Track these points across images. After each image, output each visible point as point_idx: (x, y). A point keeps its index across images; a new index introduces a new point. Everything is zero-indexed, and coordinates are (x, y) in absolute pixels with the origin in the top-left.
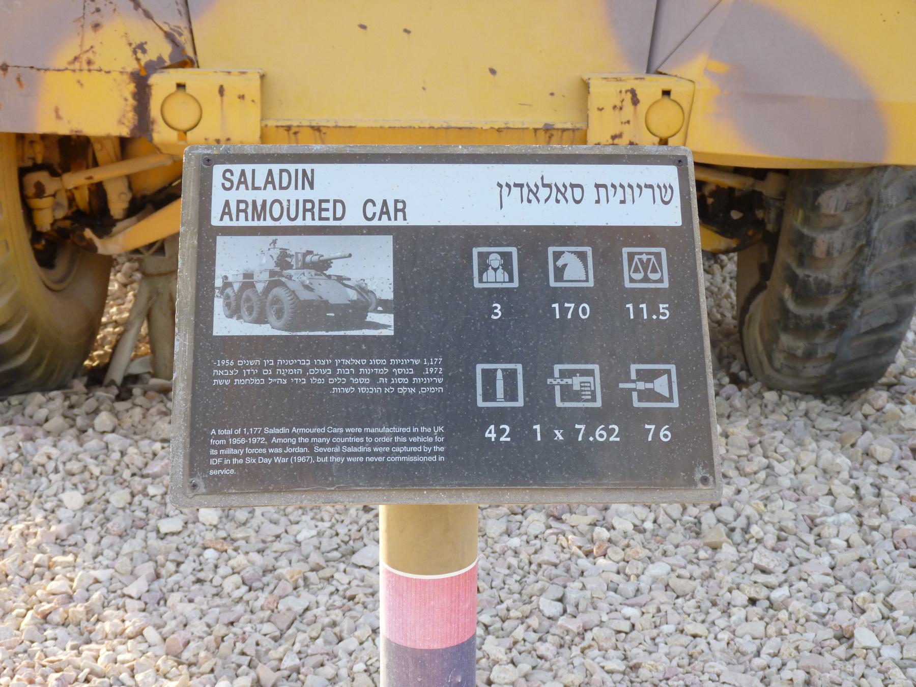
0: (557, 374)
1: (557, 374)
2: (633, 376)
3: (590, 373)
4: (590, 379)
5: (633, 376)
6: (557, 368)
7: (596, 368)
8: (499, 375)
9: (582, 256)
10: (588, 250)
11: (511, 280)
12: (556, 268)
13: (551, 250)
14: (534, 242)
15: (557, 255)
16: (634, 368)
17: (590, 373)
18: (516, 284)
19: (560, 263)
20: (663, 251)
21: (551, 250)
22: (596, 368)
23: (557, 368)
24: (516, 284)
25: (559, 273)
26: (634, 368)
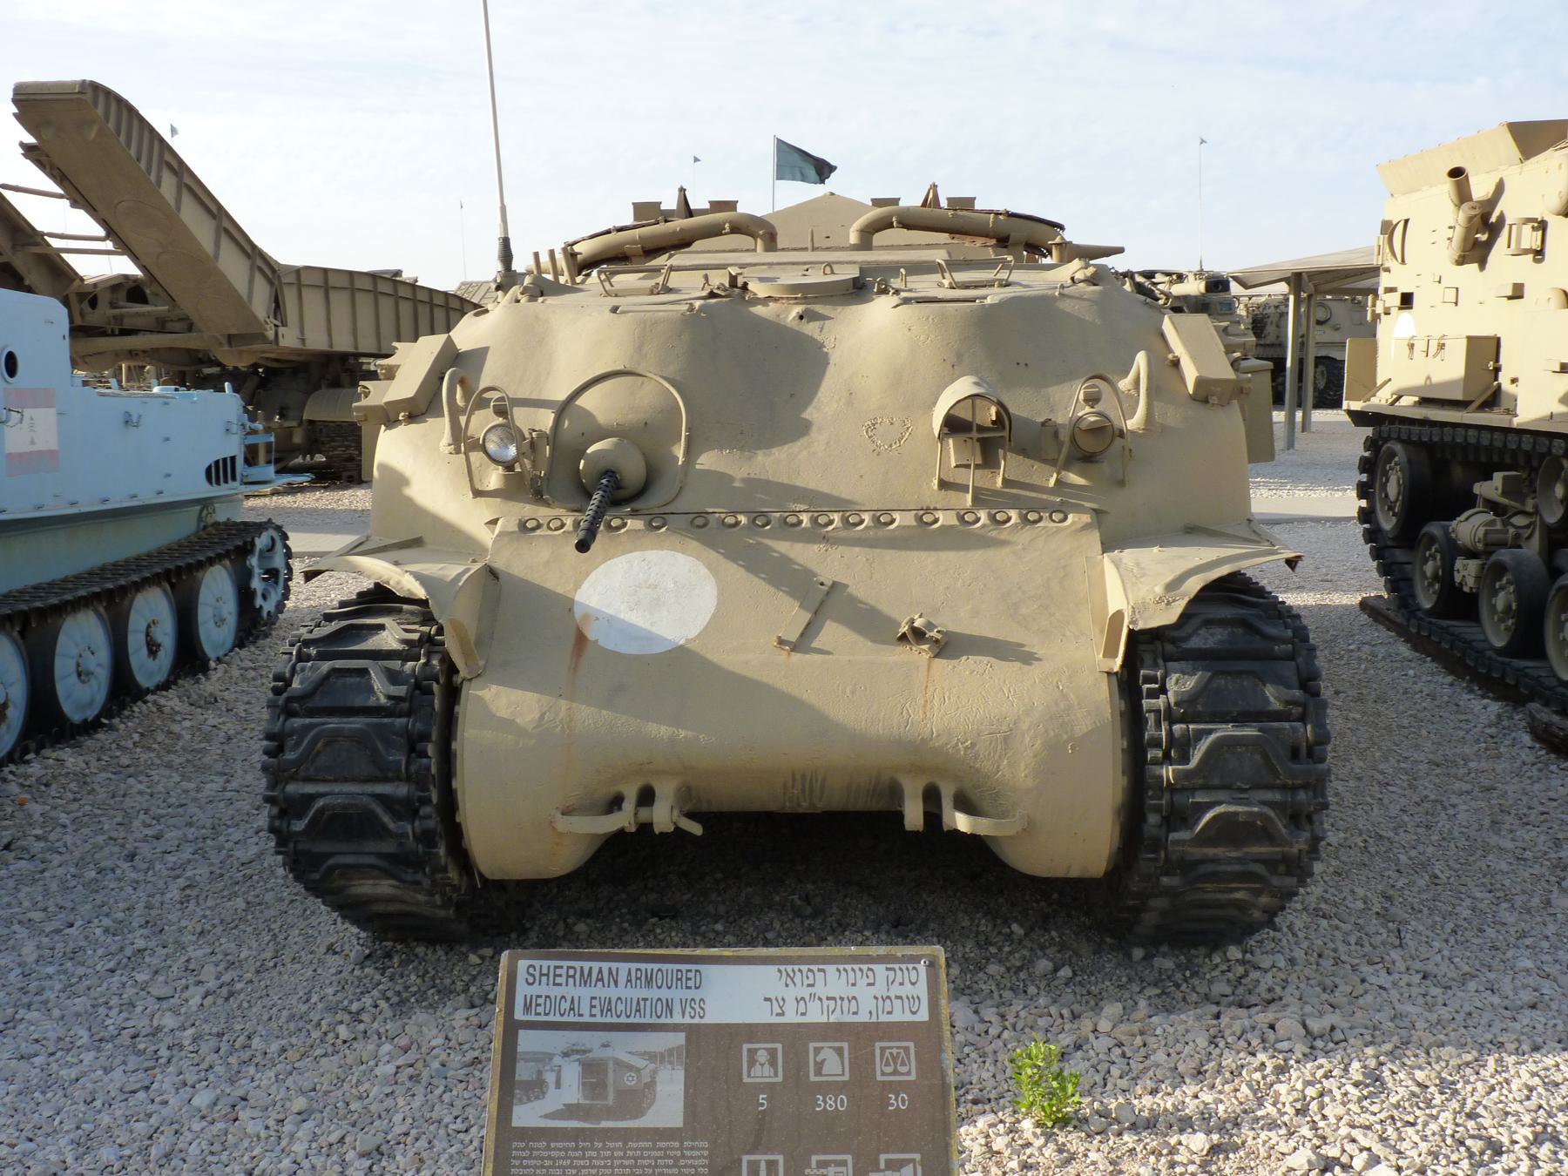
0: (814, 1165)
1: (814, 1165)
2: (882, 1166)
3: (844, 1163)
4: (843, 1169)
5: (882, 1166)
6: (814, 1158)
7: (849, 1158)
8: (763, 1166)
9: (839, 1051)
10: (845, 1045)
11: (776, 1075)
12: (816, 1063)
13: (812, 1046)
14: (795, 1038)
15: (818, 1051)
16: (883, 1158)
17: (844, 1163)
18: (780, 1079)
19: (819, 1059)
20: (911, 1045)
21: (812, 1046)
22: (849, 1158)
23: (814, 1158)
24: (780, 1079)
25: (819, 1067)
26: (883, 1158)
